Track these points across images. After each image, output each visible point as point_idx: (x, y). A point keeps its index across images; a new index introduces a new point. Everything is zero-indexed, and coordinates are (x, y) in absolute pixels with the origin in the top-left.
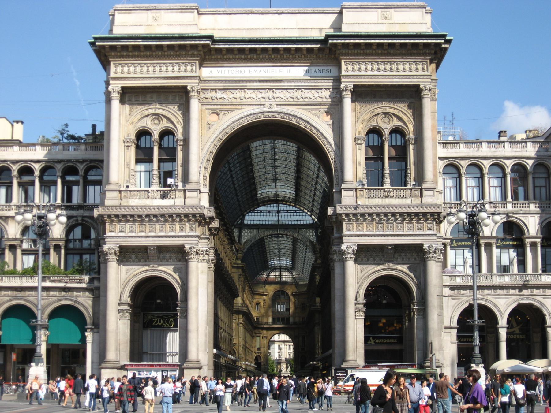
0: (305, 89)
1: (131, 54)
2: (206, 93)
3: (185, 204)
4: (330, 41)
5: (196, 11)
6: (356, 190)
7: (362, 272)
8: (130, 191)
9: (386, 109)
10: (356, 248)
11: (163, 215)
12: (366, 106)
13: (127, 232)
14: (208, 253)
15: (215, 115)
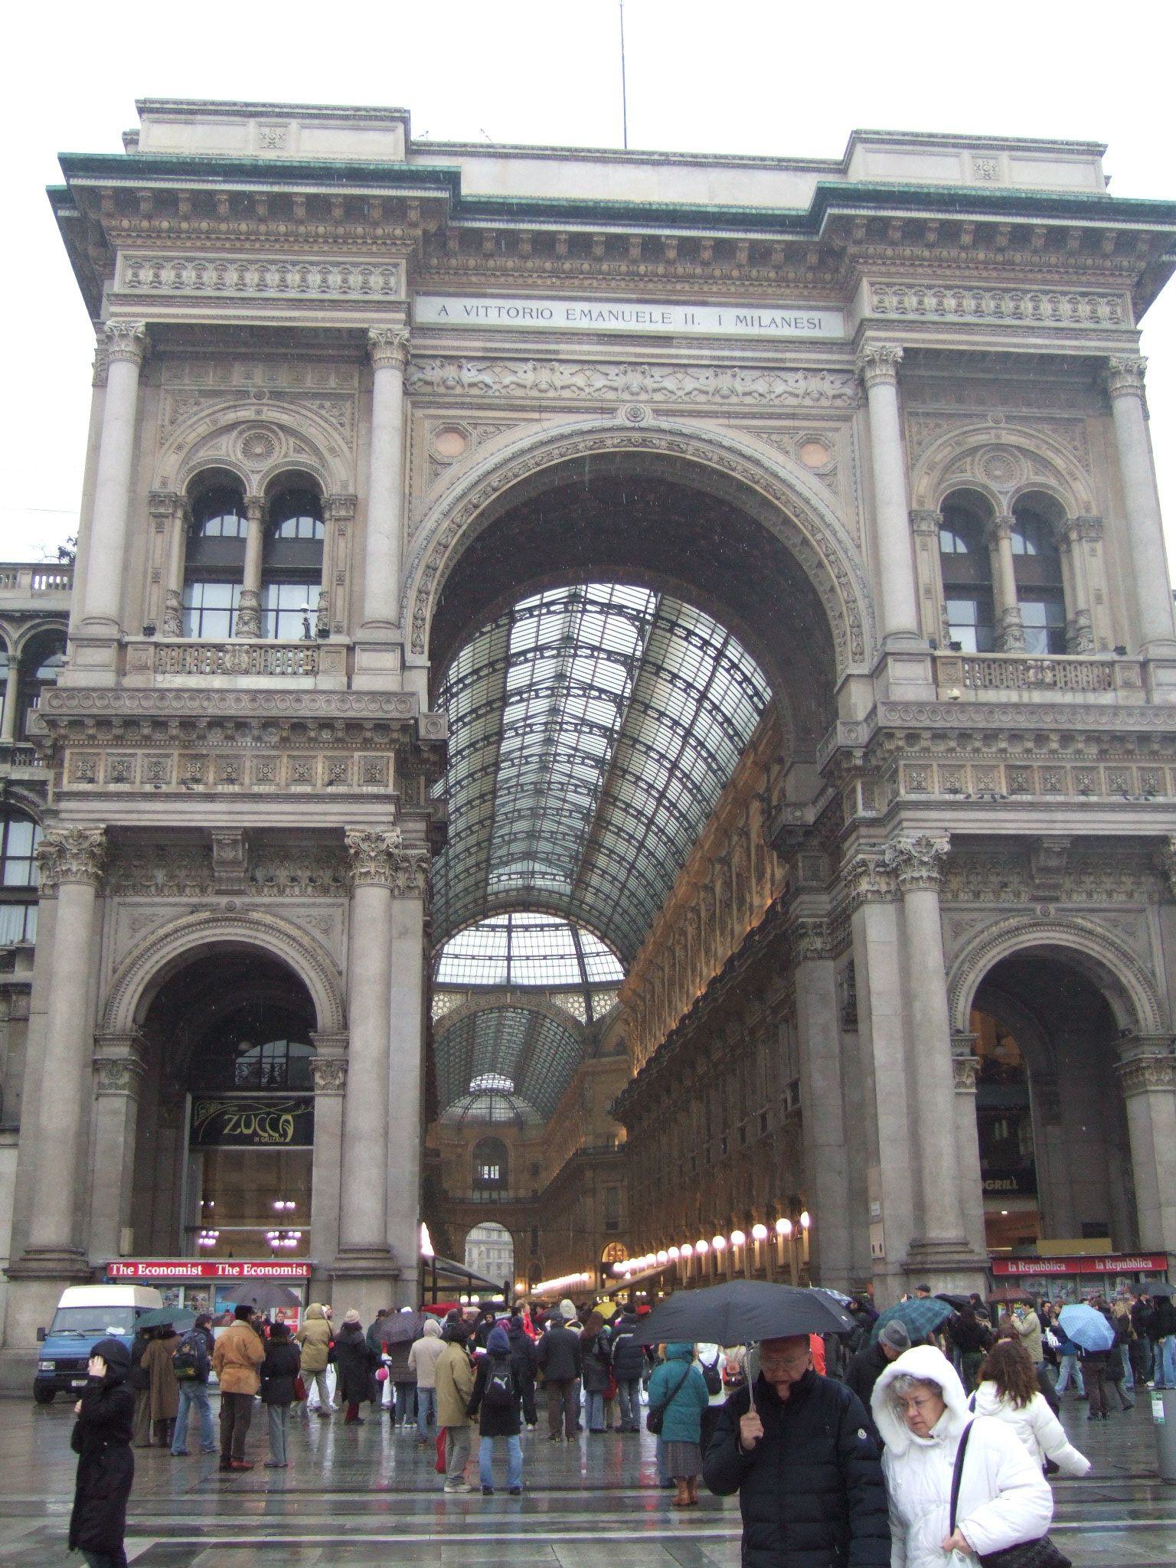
0: (741, 367)
1: (184, 225)
2: (428, 368)
3: (349, 686)
4: (830, 211)
5: (401, 128)
6: (934, 659)
7: (956, 934)
8: (157, 645)
9: (998, 437)
10: (947, 847)
11: (269, 723)
12: (938, 426)
13: (138, 779)
14: (424, 865)
15: (455, 436)
